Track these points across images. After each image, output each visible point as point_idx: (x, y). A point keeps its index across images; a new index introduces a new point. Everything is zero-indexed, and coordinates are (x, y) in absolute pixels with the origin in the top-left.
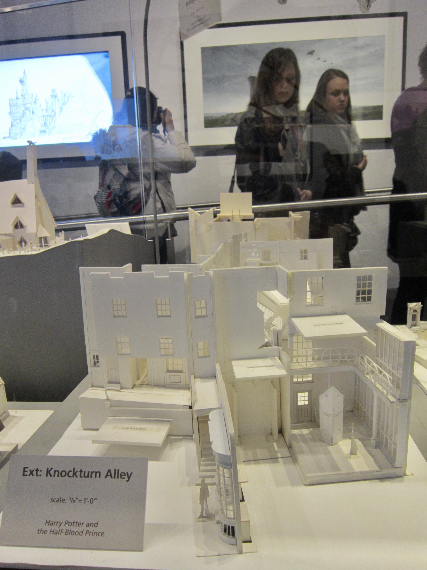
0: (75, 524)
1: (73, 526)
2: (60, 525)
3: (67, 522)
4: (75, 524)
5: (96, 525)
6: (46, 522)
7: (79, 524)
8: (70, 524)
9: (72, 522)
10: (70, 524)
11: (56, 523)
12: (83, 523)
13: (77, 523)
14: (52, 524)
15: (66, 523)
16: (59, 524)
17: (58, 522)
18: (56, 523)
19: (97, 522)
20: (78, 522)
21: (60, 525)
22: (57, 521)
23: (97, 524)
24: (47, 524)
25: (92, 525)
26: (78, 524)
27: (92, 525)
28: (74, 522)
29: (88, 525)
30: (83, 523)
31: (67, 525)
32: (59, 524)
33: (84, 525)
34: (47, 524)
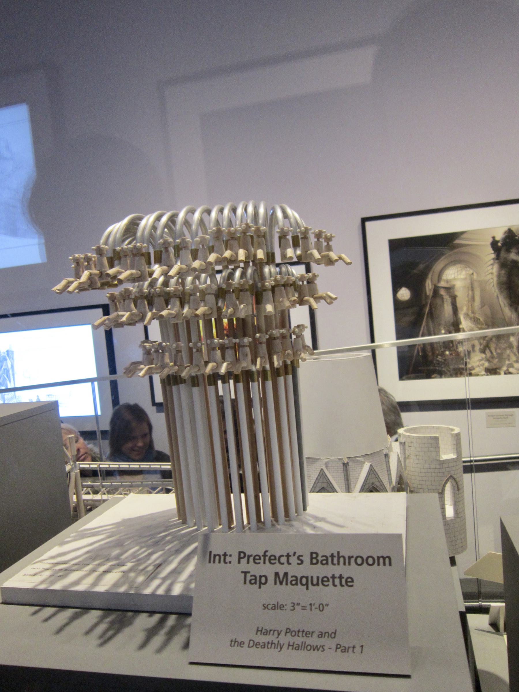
0: (300, 634)
1: (298, 636)
2: (279, 635)
3: (288, 631)
4: (300, 634)
5: (333, 635)
6: (258, 631)
7: (308, 634)
8: (293, 634)
9: (296, 630)
10: (293, 634)
11: (272, 632)
12: (313, 632)
13: (303, 631)
14: (267, 633)
15: (286, 632)
16: (276, 633)
17: (274, 631)
18: (272, 632)
19: (334, 631)
20: (306, 631)
21: (279, 635)
22: (273, 628)
23: (335, 633)
24: (259, 633)
25: (327, 634)
26: (306, 634)
27: (327, 634)
28: (299, 631)
29: (321, 635)
30: (313, 632)
31: (289, 635)
32: (276, 633)
33: (315, 635)
34: (259, 633)
